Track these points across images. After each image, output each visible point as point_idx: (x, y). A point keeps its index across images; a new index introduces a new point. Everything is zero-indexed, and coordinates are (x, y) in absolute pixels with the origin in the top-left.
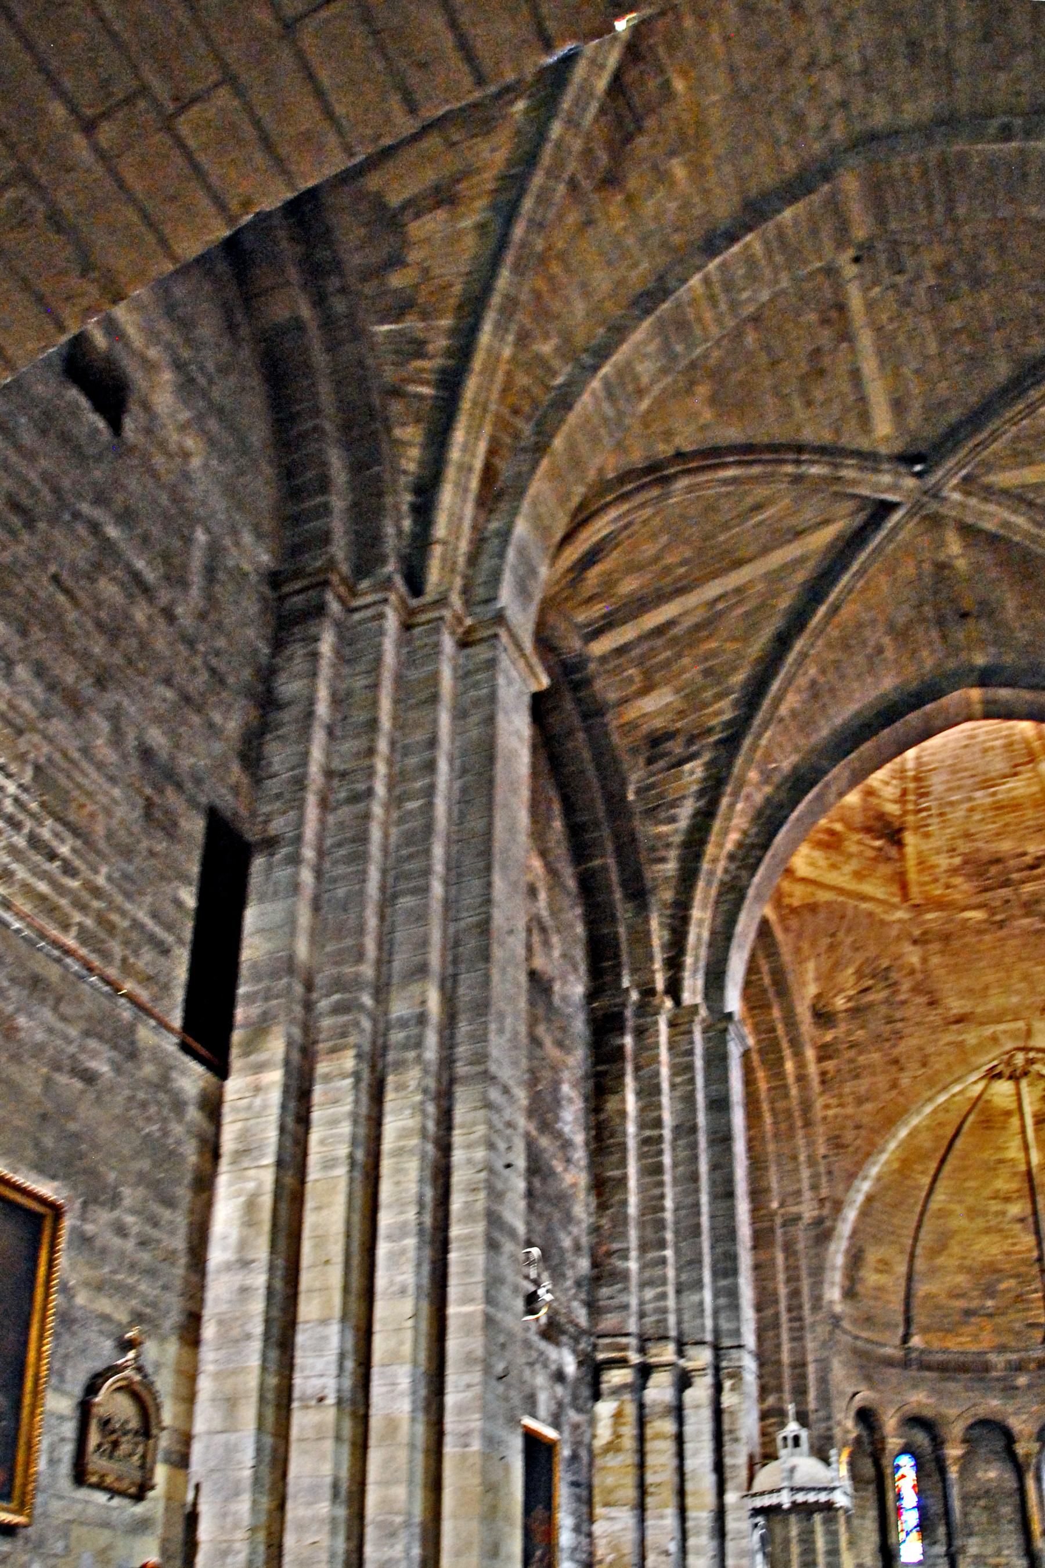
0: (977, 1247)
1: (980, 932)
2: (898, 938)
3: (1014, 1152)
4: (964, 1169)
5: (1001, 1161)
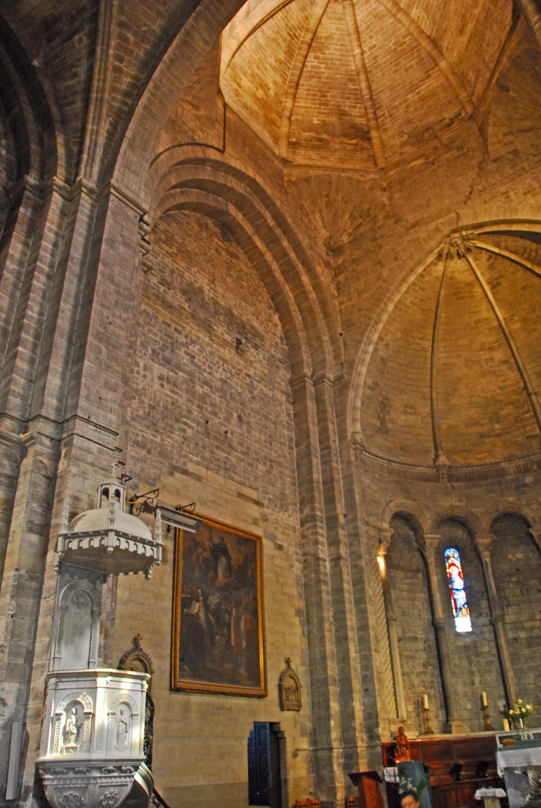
1: (420, 171)
2: (371, 188)
3: (485, 314)
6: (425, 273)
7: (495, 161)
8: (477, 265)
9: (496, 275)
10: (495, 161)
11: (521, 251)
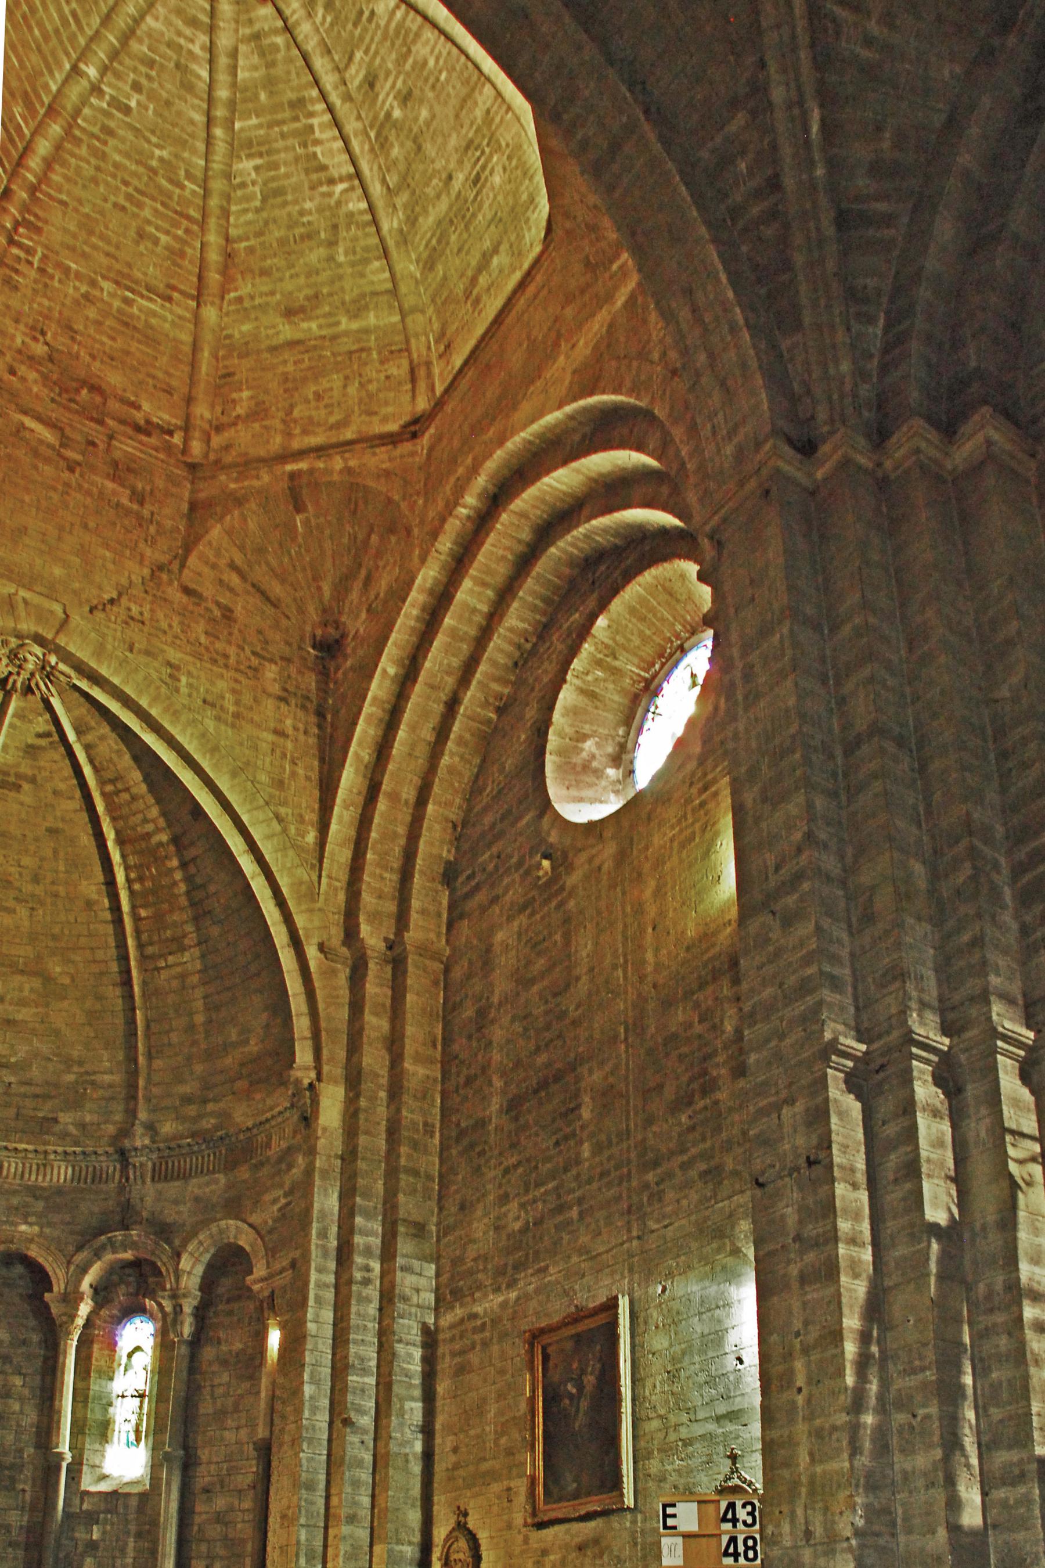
7: (187, 591)
9: (25, 769)
10: (187, 591)
11: (109, 775)
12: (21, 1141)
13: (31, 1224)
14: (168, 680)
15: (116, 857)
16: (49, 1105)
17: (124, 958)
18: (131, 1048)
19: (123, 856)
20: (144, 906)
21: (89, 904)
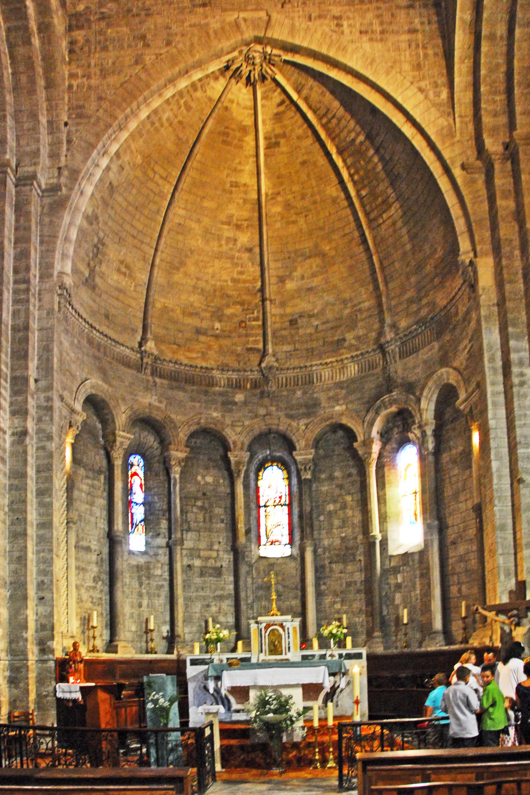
0: (210, 270)
4: (203, 185)
5: (235, 185)
6: (199, 85)
8: (263, 106)
12: (328, 358)
13: (341, 405)
14: (336, 29)
15: (339, 163)
16: (339, 332)
17: (359, 226)
18: (375, 281)
19: (344, 161)
20: (364, 187)
21: (334, 201)
